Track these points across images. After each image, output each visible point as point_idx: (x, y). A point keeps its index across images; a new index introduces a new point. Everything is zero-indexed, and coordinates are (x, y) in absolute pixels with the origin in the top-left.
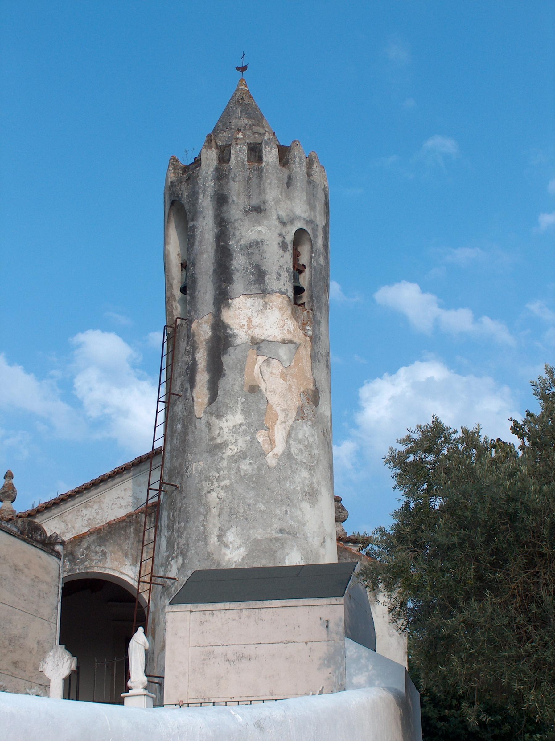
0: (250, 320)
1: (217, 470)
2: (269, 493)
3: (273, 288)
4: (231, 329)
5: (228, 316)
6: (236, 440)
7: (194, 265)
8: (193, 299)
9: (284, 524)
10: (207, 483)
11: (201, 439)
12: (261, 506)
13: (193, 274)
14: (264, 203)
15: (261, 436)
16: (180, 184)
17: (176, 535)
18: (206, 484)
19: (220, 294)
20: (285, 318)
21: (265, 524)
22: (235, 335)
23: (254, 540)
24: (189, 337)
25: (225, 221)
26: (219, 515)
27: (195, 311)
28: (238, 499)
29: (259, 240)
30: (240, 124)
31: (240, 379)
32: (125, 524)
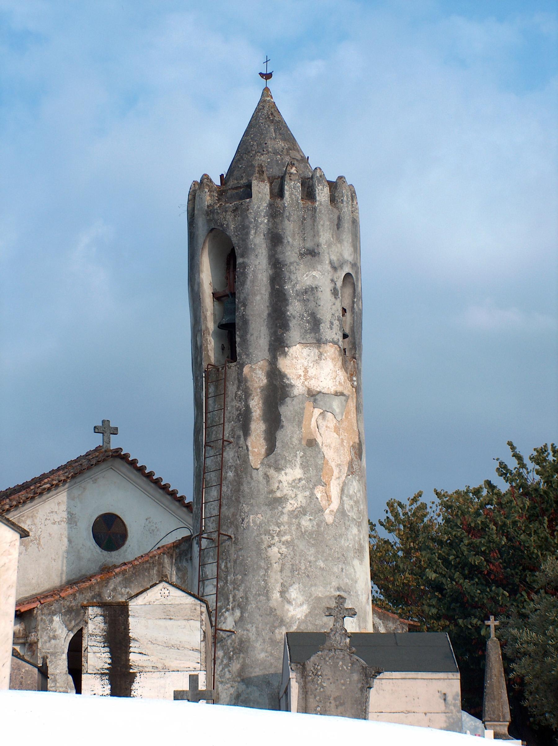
0: (306, 371)
1: (277, 524)
2: (327, 550)
3: (327, 337)
4: (288, 379)
5: (284, 364)
6: (296, 495)
7: (245, 305)
8: (244, 341)
9: (341, 582)
10: (267, 537)
11: (259, 490)
12: (321, 564)
13: (243, 315)
14: (318, 246)
15: (319, 492)
16: (224, 213)
17: (231, 587)
18: (266, 538)
19: (275, 341)
20: (337, 369)
21: (325, 582)
22: (292, 386)
23: (315, 597)
24: (240, 382)
25: (280, 263)
26: (281, 571)
27: (248, 355)
28: (300, 556)
29: (314, 286)
30: (276, 146)
31: (298, 432)
32: (148, 565)
